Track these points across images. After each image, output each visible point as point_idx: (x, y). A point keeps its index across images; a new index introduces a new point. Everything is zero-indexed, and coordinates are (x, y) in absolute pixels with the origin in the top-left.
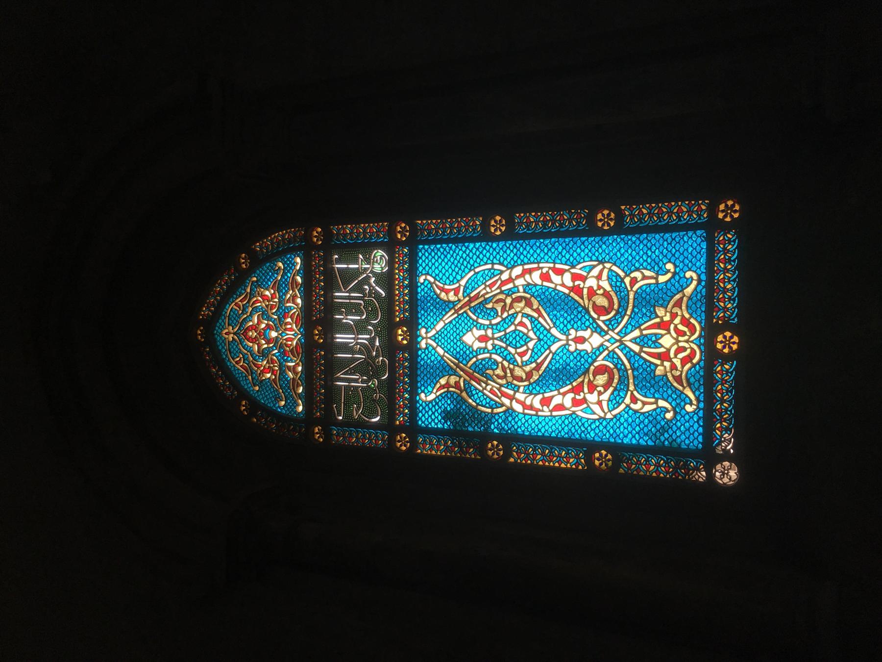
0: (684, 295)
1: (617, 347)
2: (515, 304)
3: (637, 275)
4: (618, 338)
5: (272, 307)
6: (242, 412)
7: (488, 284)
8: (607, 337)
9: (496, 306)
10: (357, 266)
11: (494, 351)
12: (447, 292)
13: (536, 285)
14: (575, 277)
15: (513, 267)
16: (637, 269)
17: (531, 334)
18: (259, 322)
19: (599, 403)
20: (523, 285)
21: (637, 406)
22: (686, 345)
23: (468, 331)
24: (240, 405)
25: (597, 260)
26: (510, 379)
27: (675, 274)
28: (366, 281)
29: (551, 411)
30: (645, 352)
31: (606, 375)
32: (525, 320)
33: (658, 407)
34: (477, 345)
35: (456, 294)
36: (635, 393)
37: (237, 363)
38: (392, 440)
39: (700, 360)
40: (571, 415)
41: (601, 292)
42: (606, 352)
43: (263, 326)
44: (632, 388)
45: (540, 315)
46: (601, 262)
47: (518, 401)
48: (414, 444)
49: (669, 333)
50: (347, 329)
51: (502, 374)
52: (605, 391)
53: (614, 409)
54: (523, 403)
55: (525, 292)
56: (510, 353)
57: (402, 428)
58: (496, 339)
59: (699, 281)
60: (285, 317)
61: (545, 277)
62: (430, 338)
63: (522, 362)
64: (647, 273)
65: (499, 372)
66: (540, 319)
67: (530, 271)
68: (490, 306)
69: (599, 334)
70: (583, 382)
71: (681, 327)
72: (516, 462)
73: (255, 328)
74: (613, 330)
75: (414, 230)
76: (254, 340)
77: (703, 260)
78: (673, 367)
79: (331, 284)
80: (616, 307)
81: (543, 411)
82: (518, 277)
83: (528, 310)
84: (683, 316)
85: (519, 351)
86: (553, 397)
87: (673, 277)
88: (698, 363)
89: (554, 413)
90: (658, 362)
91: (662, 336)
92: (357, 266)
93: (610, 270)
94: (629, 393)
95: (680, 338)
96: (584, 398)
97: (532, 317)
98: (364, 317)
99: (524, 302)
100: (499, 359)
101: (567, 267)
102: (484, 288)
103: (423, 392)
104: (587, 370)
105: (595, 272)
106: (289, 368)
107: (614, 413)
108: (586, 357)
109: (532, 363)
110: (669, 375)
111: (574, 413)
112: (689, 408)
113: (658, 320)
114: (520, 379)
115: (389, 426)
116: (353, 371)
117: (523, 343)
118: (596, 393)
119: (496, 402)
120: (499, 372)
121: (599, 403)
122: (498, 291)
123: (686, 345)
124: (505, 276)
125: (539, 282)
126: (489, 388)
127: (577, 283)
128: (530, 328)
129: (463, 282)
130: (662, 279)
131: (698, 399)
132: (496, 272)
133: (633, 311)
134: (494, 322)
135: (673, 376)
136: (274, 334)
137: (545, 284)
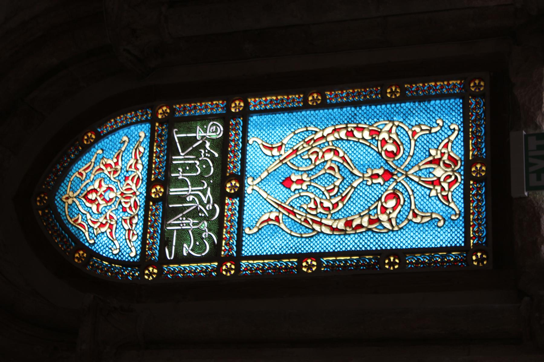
0: (449, 140)
10: (194, 135)
14: (372, 132)
17: (338, 176)
18: (100, 186)
19: (390, 220)
20: (332, 141)
21: (418, 220)
28: (203, 146)
30: (423, 181)
32: (333, 166)
33: (432, 219)
41: (391, 141)
44: (413, 207)
46: (390, 121)
49: (439, 165)
50: (183, 183)
51: (314, 207)
55: (333, 145)
59: (459, 130)
60: (126, 178)
61: (350, 134)
63: (331, 197)
64: (424, 127)
65: (312, 205)
66: (345, 164)
71: (447, 162)
73: (95, 190)
75: (247, 104)
76: (92, 201)
78: (443, 189)
79: (172, 150)
83: (336, 158)
86: (352, 220)
90: (431, 187)
97: (339, 162)
98: (198, 173)
99: (332, 153)
100: (312, 196)
104: (380, 199)
105: (387, 128)
106: (125, 220)
107: (401, 226)
110: (439, 195)
112: (453, 217)
114: (328, 209)
116: (187, 216)
124: (319, 135)
130: (433, 130)
135: (443, 196)
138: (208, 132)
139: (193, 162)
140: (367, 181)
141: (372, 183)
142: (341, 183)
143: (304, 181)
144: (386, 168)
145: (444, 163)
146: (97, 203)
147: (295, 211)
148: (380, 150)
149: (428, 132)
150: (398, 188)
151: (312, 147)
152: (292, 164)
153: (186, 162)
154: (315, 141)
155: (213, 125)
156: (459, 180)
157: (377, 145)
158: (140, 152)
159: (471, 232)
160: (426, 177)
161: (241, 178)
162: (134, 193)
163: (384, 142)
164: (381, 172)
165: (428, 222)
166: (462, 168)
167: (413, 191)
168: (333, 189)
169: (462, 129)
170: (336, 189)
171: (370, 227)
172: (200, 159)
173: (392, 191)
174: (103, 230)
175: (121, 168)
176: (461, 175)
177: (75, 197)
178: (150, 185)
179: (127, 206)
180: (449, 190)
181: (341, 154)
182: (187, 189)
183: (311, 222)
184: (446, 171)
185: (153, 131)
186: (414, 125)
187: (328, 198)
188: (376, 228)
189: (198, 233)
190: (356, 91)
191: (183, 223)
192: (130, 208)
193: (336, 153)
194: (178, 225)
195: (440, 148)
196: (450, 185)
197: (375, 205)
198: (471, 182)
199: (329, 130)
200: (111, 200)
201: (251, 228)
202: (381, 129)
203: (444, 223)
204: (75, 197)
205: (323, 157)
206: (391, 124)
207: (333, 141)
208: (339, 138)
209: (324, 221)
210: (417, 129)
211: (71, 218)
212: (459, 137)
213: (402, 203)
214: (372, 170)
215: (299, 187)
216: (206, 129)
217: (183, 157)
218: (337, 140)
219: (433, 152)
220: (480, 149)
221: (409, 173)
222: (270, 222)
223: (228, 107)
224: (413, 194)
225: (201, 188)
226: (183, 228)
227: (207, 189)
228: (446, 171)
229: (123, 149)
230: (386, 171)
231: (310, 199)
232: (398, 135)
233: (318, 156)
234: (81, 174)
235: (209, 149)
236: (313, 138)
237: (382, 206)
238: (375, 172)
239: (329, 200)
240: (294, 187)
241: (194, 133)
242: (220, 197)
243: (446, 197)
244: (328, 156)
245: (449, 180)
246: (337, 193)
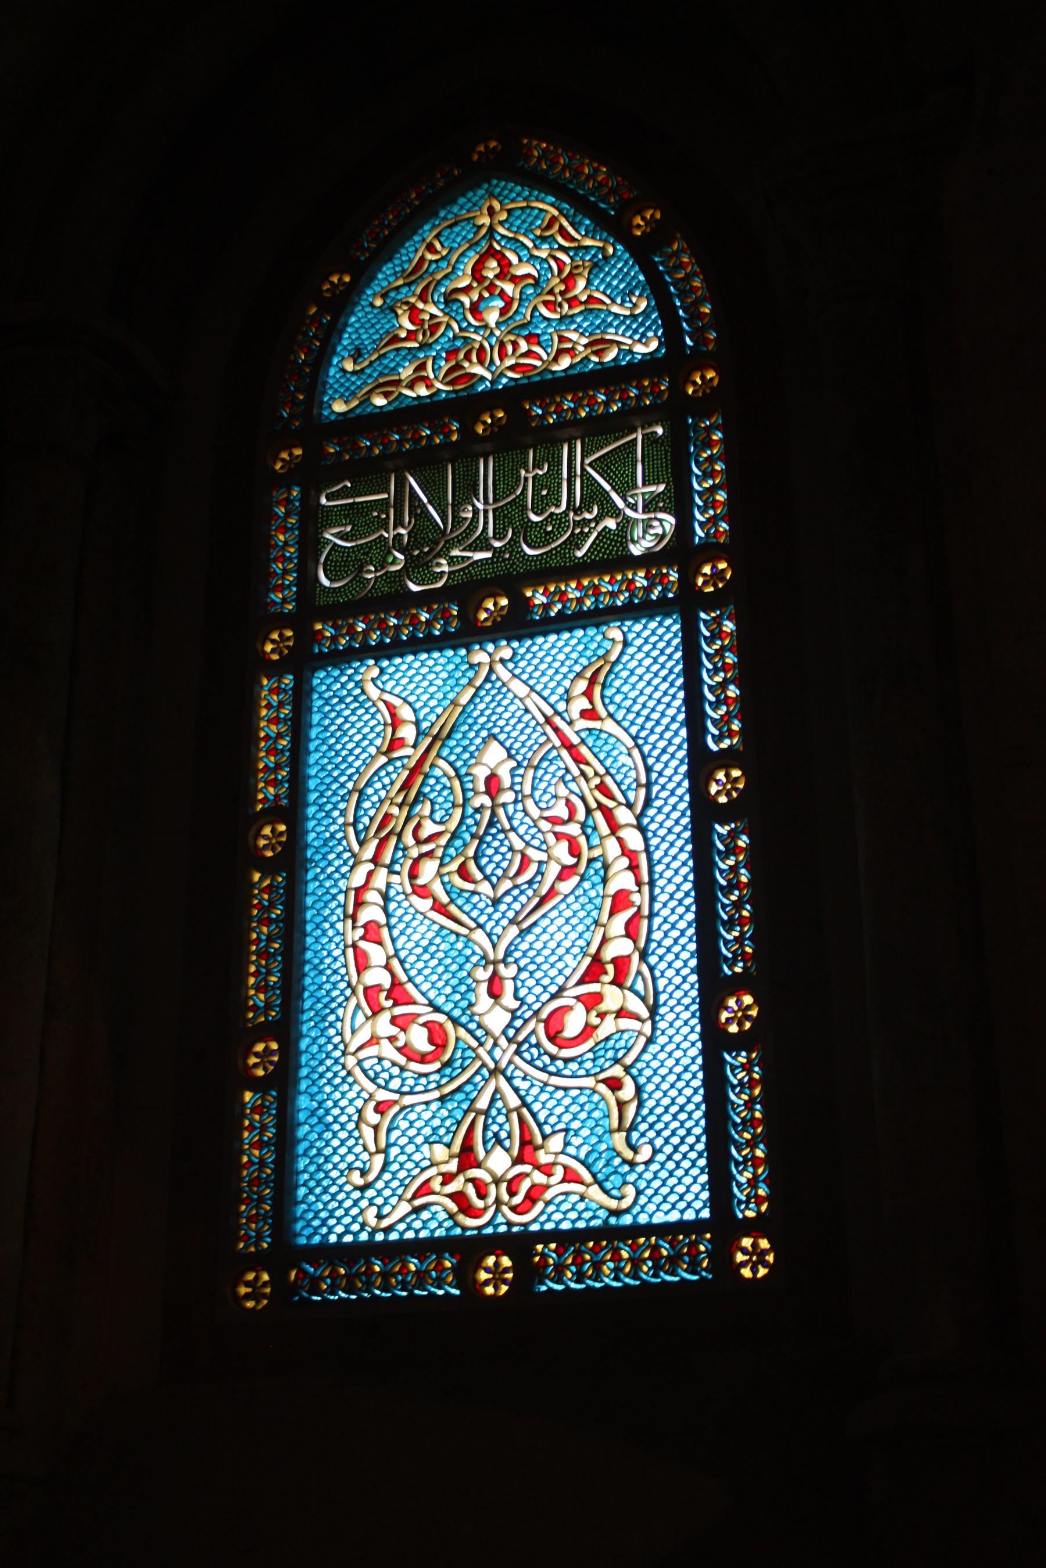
0: (588, 1186)
1: (484, 1065)
2: (564, 845)
3: (628, 1092)
6: (326, 279)
7: (608, 780)
8: (503, 1042)
11: (470, 811)
12: (588, 694)
14: (621, 963)
15: (642, 829)
16: (639, 1089)
19: (374, 1040)
22: (491, 1200)
23: (508, 750)
24: (342, 272)
26: (414, 853)
27: (632, 1164)
29: (354, 946)
32: (533, 869)
34: (481, 773)
35: (585, 714)
37: (431, 248)
38: (282, 621)
39: (465, 1229)
40: (349, 985)
41: (595, 1021)
42: (474, 1044)
43: (509, 288)
46: (653, 1010)
47: (370, 874)
48: (275, 670)
51: (424, 834)
52: (400, 1050)
53: (364, 1071)
54: (365, 887)
55: (590, 861)
56: (465, 845)
57: (306, 637)
58: (493, 814)
59: (617, 1213)
61: (620, 901)
62: (491, 670)
67: (633, 867)
69: (509, 1025)
70: (414, 1003)
71: (525, 1186)
72: (253, 885)
74: (518, 1052)
76: (477, 273)
77: (659, 1219)
78: (448, 1178)
80: (566, 1053)
81: (354, 928)
83: (554, 870)
84: (547, 1187)
87: (625, 1161)
88: (457, 1224)
89: (350, 952)
90: (456, 1148)
91: (507, 1150)
95: (504, 1185)
96: (382, 1009)
99: (572, 861)
102: (596, 774)
103: (382, 671)
106: (422, 367)
108: (464, 1004)
109: (448, 893)
110: (433, 1171)
111: (354, 992)
115: (311, 605)
117: (488, 871)
118: (394, 1030)
119: (367, 829)
121: (374, 1040)
122: (594, 805)
123: (491, 1200)
124: (624, 816)
125: (613, 888)
126: (395, 810)
127: (610, 968)
128: (520, 880)
131: (388, 1230)
132: (631, 795)
133: (557, 1088)
134: (530, 804)
137: (608, 902)
146: (475, 285)
182: (491, 500)
193: (565, 873)
202: (631, 989)
205: (558, 836)
210: (628, 1092)
218: (606, 867)
225: (491, 533)
227: (488, 547)
233: (564, 823)
239: (439, 875)
244: (561, 851)
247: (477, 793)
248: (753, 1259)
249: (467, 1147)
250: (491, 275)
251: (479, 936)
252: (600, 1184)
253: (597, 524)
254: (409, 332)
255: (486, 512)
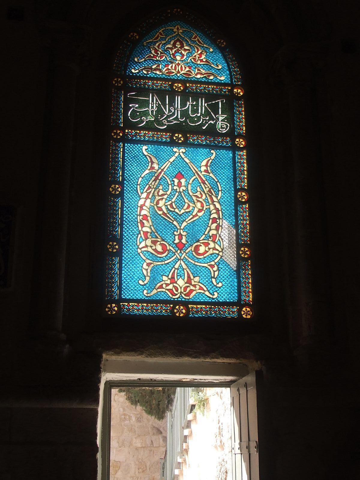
1: (177, 257)
3: (215, 269)
4: (182, 258)
5: (195, 59)
9: (199, 193)
10: (220, 113)
12: (206, 166)
13: (210, 215)
15: (220, 204)
17: (183, 211)
20: (210, 208)
22: (179, 291)
25: (223, 248)
28: (211, 118)
30: (174, 271)
31: (162, 251)
32: (191, 208)
36: (152, 265)
41: (207, 250)
42: (174, 251)
43: (183, 52)
45: (194, 217)
46: (222, 249)
47: (145, 201)
49: (186, 283)
50: (183, 104)
51: (160, 194)
52: (153, 250)
54: (144, 205)
55: (206, 209)
59: (213, 299)
62: (179, 154)
63: (167, 206)
64: (216, 273)
65: (161, 192)
66: (191, 216)
68: (198, 189)
71: (188, 289)
73: (182, 46)
74: (186, 255)
75: (241, 149)
78: (167, 285)
79: (209, 97)
82: (215, 205)
83: (196, 210)
85: (173, 204)
86: (148, 221)
90: (170, 277)
91: (184, 280)
92: (220, 113)
93: (218, 255)
94: (152, 262)
98: (190, 115)
99: (201, 208)
100: (168, 193)
101: (220, 232)
104: (163, 240)
105: (217, 247)
106: (159, 66)
107: (141, 254)
110: (163, 282)
111: (140, 233)
112: (145, 292)
113: (192, 277)
114: (158, 203)
116: (159, 107)
120: (161, 192)
124: (215, 199)
125: (211, 217)
129: (211, 175)
130: (214, 280)
135: (162, 284)
136: (178, 58)
137: (211, 220)
138: (222, 122)
139: (200, 112)
140: (177, 232)
141: (175, 235)
142: (177, 213)
143: (180, 188)
144: (186, 245)
145: (188, 286)
147: (158, 181)
148: (201, 242)
149: (213, 275)
150: (170, 253)
151: (206, 194)
152: (194, 180)
153: (200, 107)
154: (210, 196)
155: (227, 126)
156: (174, 297)
157: (205, 240)
158: (209, 76)
159: (133, 304)
160: (177, 274)
161: (185, 144)
162: (179, 72)
163: (207, 244)
164: (184, 241)
165: (143, 273)
166: (183, 300)
167: (168, 263)
168: (173, 208)
169: (213, 301)
170: (173, 210)
171: (142, 233)
172: (201, 117)
173: (168, 249)
174: (153, 52)
175: (198, 64)
176: (177, 298)
177: (178, 33)
178: (183, 82)
179: (170, 67)
180: (166, 289)
181: (200, 214)
182: (179, 108)
183: (148, 191)
184: (181, 288)
185: (225, 84)
186: (219, 266)
187: (166, 204)
188: (141, 236)
189: (146, 114)
190: (248, 226)
191: (153, 104)
192: (168, 69)
193: (200, 211)
194: (153, 101)
195: (200, 284)
196: (171, 291)
197: (159, 237)
198: (172, 306)
199: (218, 206)
200: (175, 57)
201: (147, 151)
202: (216, 243)
203: (141, 285)
204: (178, 33)
205: (198, 201)
206: (220, 250)
207: (210, 209)
208: (212, 213)
209: (149, 201)
210: (215, 269)
211: (163, 31)
212: (208, 298)
213: (159, 256)
214: (185, 236)
215: (176, 184)
216: (225, 122)
217: (204, 105)
218: (210, 212)
219: (197, 279)
220: (197, 312)
221: (182, 262)
222: (150, 164)
223: (240, 136)
224: (165, 264)
226: (150, 105)
228: (181, 288)
229: (212, 65)
230: (185, 244)
231: (166, 192)
232: (211, 254)
234: (195, 38)
235: (209, 123)
236: (213, 194)
237: (159, 241)
238: (184, 238)
240: (176, 181)
241: (221, 113)
242: (172, 129)
243: (161, 287)
244: (199, 205)
245: (174, 290)
246: (169, 210)
247: (175, 185)
248: (247, 313)
249: (173, 277)
250: (179, 46)
251: (175, 223)
252: (209, 291)
253: (209, 121)
254: (154, 55)
255: (178, 111)
